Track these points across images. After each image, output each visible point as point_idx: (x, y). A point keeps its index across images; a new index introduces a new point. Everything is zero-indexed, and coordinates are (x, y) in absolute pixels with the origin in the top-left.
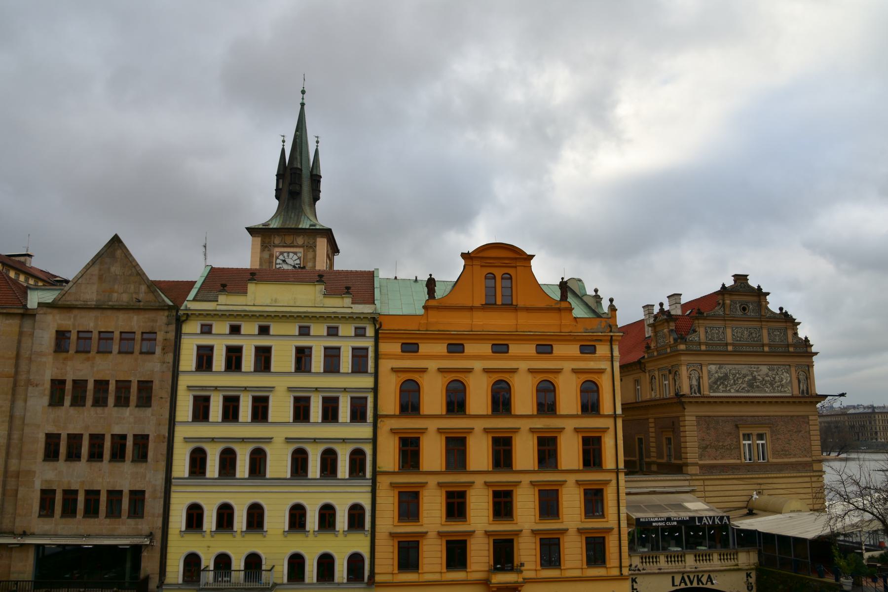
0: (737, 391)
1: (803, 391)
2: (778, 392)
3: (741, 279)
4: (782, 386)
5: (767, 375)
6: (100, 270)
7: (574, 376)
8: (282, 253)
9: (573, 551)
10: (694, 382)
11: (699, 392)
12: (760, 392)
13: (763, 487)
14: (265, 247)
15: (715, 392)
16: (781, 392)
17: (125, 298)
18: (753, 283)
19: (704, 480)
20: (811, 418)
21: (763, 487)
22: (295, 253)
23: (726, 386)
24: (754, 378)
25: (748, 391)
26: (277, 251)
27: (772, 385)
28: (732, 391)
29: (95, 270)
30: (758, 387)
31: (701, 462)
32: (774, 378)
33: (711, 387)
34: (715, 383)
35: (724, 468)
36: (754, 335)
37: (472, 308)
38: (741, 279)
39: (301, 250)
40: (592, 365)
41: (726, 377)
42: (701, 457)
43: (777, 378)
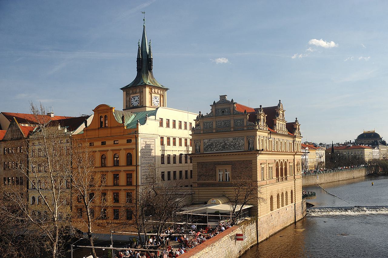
0: (217, 150)
1: (251, 148)
2: (237, 149)
3: (223, 97)
4: (240, 147)
5: (232, 142)
6: (11, 129)
7: (125, 151)
8: (133, 97)
9: (123, 214)
10: (198, 148)
11: (200, 152)
12: (228, 150)
13: (225, 193)
14: (128, 95)
15: (206, 151)
16: (239, 149)
17: (16, 137)
18: (228, 99)
19: (199, 189)
20: (253, 161)
21: (225, 193)
22: (137, 96)
23: (212, 148)
24: (226, 144)
25: (222, 150)
26: (132, 96)
27: (234, 146)
28: (214, 150)
29: (10, 129)
30: (227, 148)
31: (198, 182)
32: (236, 143)
33: (205, 149)
34: (207, 147)
35: (208, 185)
36: (227, 124)
37: (95, 129)
38: (223, 97)
39: (139, 94)
40: (130, 147)
41: (212, 144)
42: (198, 180)
43: (237, 143)
